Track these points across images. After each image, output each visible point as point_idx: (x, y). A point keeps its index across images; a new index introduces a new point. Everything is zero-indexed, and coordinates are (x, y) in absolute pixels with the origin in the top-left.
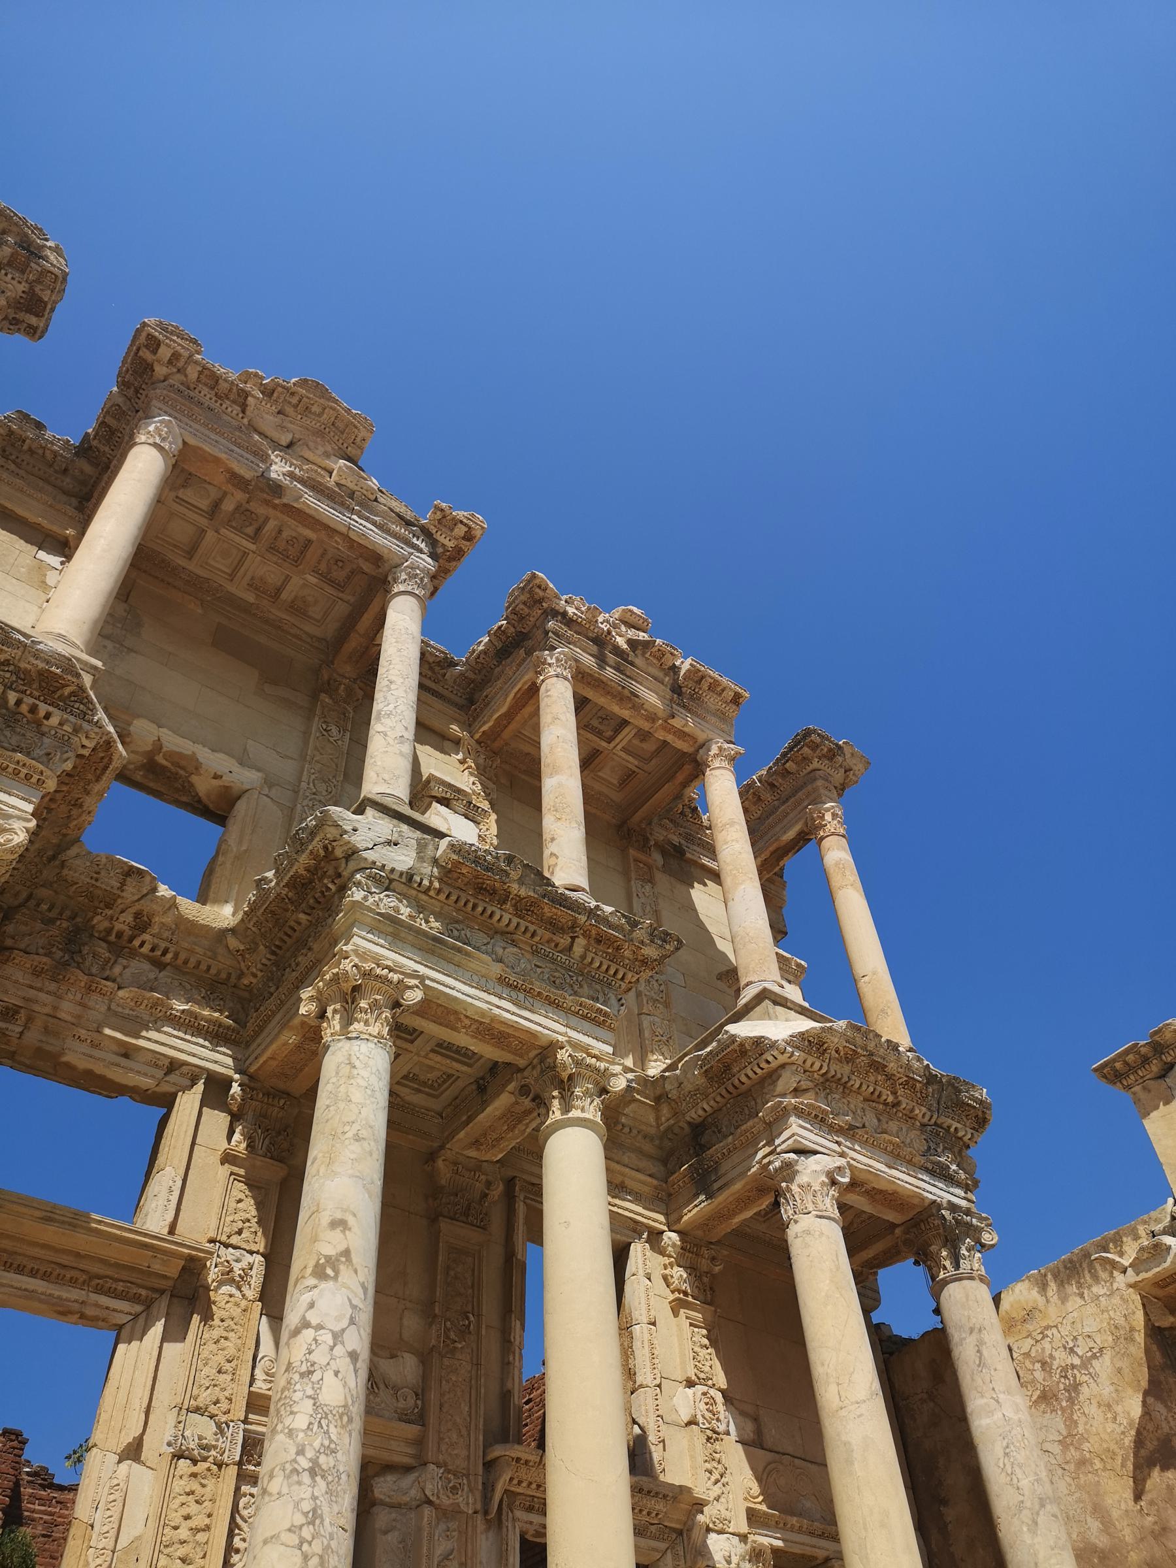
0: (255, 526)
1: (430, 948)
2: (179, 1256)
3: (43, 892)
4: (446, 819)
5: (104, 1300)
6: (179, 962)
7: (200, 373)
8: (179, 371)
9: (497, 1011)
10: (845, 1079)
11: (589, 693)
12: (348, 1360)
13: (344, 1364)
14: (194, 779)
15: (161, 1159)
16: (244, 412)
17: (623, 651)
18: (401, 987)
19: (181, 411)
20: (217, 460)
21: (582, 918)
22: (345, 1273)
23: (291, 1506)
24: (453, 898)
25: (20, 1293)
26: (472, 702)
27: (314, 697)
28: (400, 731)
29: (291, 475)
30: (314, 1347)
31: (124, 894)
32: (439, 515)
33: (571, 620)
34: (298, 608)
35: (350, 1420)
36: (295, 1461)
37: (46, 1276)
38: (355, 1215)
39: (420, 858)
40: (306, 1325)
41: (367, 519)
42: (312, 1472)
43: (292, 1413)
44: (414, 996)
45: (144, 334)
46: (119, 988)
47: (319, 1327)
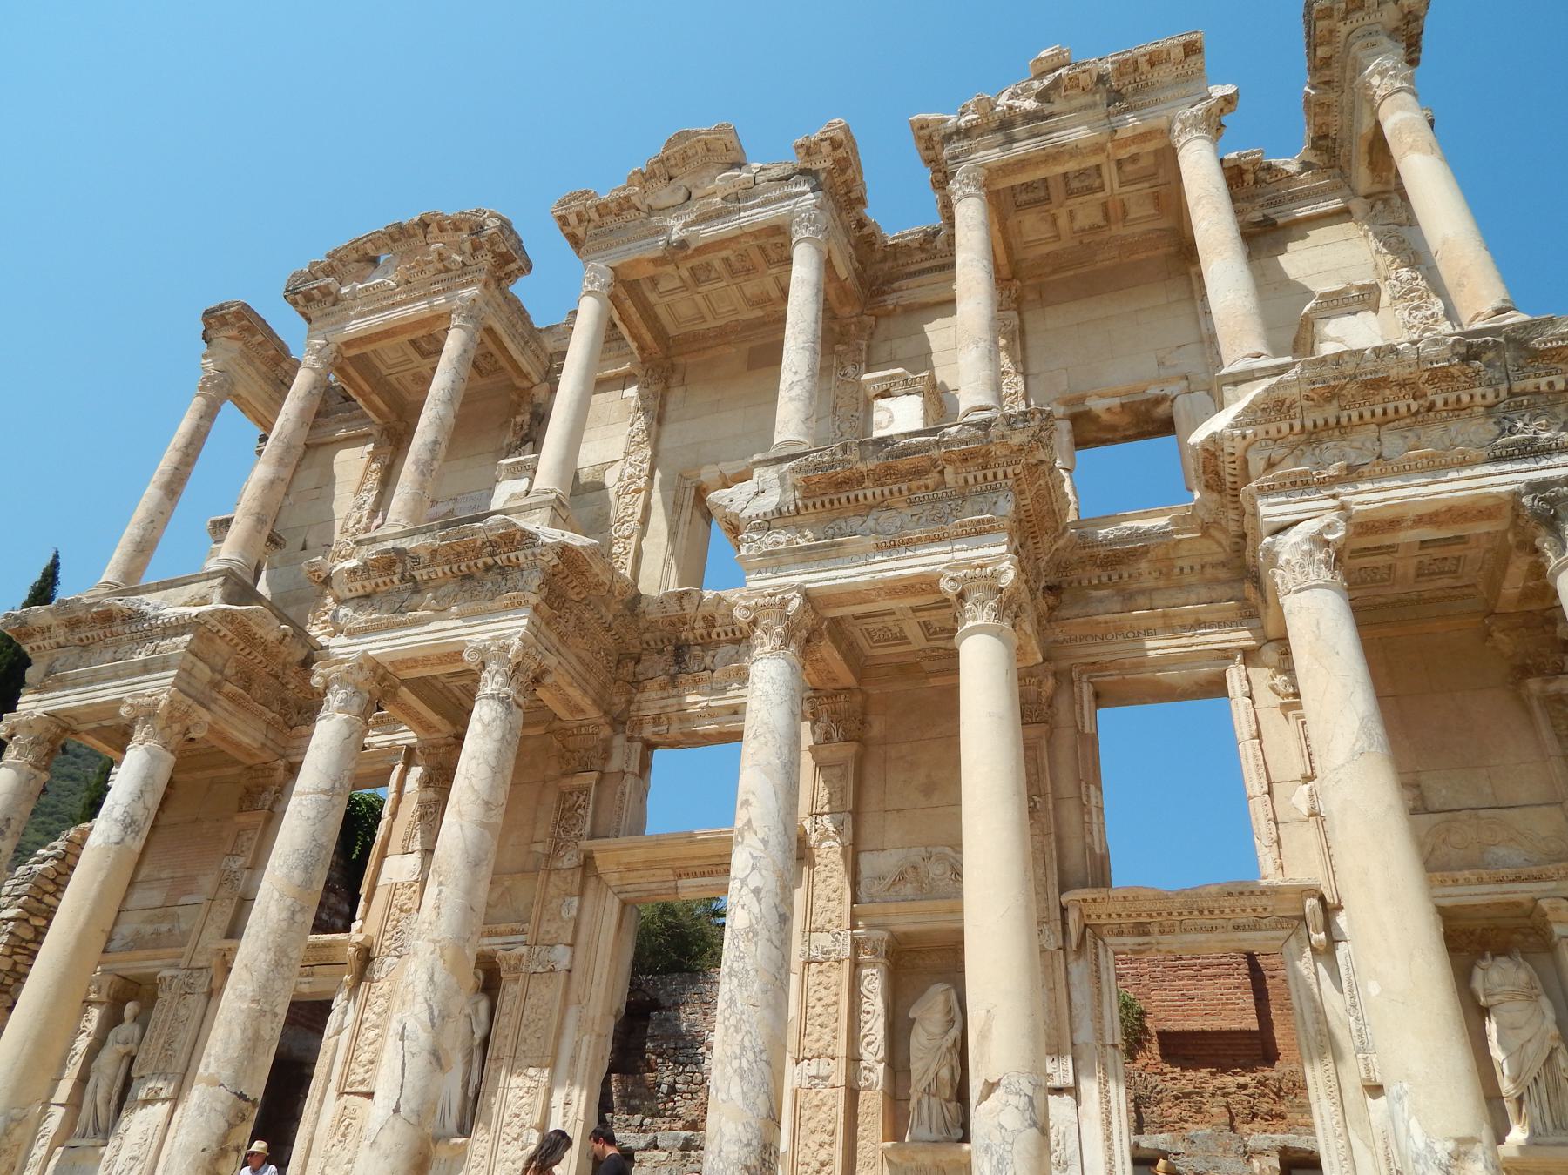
1: (806, 556)
3: (647, 636)
4: (887, 410)
9: (879, 575)
10: (1332, 421)
13: (749, 899)
17: (1035, 111)
18: (784, 603)
20: (638, 261)
21: (935, 453)
24: (819, 505)
29: (686, 225)
33: (967, 130)
35: (756, 934)
37: (711, 874)
39: (784, 491)
41: (752, 207)
42: (730, 975)
44: (795, 604)
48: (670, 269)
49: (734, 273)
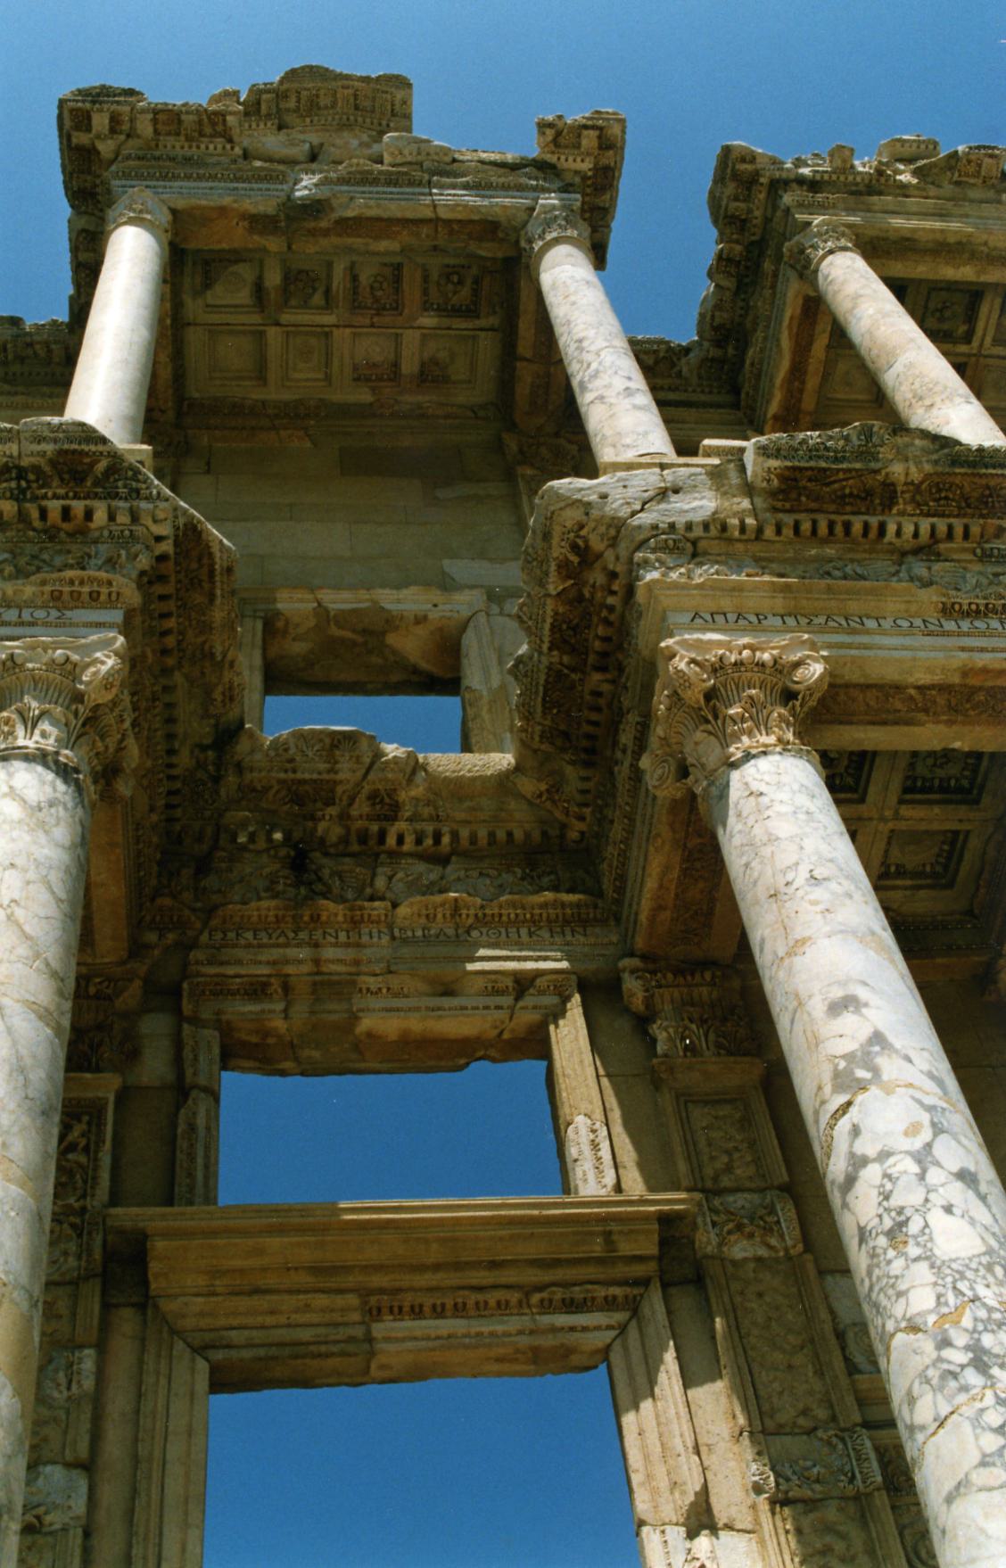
0: (321, 290)
2: (646, 1217)
5: (563, 1320)
6: (465, 843)
7: (155, 121)
8: (128, 136)
11: (899, 269)
12: (959, 1185)
13: (957, 1193)
14: (391, 639)
15: (565, 1111)
16: (230, 141)
19: (151, 177)
20: (222, 211)
22: (890, 1067)
23: (967, 1428)
25: (431, 1344)
26: (736, 390)
27: (510, 476)
28: (619, 384)
30: (889, 1186)
31: (341, 776)
32: (550, 133)
34: (431, 375)
36: (940, 1359)
37: (459, 1310)
38: (865, 984)
40: (863, 1162)
41: (454, 187)
43: (900, 1294)
45: (66, 114)
46: (395, 905)
47: (884, 1155)
48: (274, 244)
49: (356, 305)
